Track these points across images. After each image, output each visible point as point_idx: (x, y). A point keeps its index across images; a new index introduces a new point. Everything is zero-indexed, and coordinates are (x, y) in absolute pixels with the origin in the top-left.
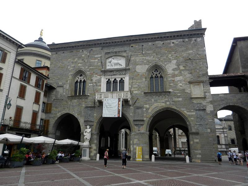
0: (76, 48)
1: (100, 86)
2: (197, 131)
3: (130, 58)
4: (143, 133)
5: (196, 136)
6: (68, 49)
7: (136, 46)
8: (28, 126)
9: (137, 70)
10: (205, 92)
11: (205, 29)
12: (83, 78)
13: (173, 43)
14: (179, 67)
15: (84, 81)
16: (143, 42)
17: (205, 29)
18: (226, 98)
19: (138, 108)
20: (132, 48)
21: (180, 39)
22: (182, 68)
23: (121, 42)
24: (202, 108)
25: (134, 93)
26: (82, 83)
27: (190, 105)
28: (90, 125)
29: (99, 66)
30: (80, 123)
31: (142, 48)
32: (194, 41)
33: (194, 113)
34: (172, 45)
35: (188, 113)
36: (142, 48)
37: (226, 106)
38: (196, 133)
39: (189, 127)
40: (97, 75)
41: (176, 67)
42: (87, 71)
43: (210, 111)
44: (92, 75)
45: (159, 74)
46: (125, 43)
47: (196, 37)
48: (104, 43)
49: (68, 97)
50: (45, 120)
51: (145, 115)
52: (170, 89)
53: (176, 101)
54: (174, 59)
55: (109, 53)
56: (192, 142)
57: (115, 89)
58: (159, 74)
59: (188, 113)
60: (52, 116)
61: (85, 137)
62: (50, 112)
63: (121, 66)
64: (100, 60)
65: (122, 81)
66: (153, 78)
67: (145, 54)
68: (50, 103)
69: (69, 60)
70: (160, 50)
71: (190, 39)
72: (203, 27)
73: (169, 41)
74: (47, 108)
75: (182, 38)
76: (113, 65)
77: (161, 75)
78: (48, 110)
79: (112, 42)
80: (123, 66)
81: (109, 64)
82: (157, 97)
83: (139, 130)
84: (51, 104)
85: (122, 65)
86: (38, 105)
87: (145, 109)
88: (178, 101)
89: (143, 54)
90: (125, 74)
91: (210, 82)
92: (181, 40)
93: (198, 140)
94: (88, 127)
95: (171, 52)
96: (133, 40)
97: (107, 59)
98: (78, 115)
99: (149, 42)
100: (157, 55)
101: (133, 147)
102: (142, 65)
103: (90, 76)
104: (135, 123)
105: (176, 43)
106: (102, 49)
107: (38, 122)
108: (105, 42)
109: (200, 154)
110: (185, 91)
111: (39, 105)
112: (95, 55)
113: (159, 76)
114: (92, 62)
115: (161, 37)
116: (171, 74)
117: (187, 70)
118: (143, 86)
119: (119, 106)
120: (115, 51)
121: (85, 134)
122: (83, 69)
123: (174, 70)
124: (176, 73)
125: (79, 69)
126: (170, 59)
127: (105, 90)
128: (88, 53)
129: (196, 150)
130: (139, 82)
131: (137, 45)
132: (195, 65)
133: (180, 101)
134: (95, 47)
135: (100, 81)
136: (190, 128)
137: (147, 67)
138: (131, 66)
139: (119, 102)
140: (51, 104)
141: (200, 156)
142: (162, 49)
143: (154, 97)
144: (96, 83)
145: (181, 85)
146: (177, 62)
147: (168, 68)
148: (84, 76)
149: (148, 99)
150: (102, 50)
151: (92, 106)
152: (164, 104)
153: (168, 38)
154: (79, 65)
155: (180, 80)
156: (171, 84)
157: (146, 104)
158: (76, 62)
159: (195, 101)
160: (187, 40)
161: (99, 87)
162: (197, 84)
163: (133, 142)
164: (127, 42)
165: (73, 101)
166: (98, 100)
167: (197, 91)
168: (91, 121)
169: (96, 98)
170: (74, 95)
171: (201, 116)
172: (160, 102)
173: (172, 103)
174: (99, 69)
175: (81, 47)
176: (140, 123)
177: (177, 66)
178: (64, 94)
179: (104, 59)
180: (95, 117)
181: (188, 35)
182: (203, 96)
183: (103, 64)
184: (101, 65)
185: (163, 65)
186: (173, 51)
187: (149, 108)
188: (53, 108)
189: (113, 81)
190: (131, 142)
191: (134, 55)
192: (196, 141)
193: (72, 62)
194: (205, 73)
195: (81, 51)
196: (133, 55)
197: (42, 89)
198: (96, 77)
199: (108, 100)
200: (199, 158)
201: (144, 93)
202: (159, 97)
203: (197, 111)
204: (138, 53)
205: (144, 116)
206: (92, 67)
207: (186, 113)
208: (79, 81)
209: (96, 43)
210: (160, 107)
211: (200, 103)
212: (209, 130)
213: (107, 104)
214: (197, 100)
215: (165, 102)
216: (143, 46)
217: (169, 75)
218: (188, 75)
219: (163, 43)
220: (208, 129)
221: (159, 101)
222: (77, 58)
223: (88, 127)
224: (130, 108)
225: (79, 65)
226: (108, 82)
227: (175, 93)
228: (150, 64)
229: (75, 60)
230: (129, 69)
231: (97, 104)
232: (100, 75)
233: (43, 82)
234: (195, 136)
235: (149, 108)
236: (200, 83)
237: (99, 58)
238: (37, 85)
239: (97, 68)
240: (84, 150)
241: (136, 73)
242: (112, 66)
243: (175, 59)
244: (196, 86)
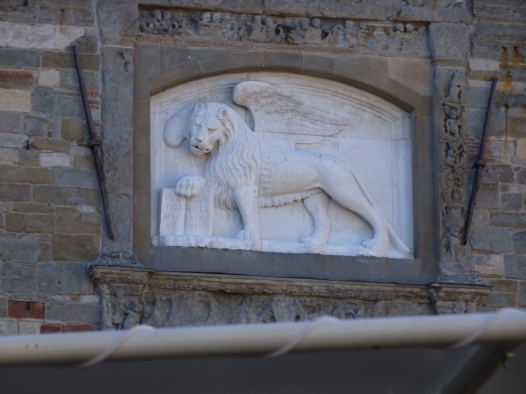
64: (72, 102)
76: (248, 197)
184: (90, 184)
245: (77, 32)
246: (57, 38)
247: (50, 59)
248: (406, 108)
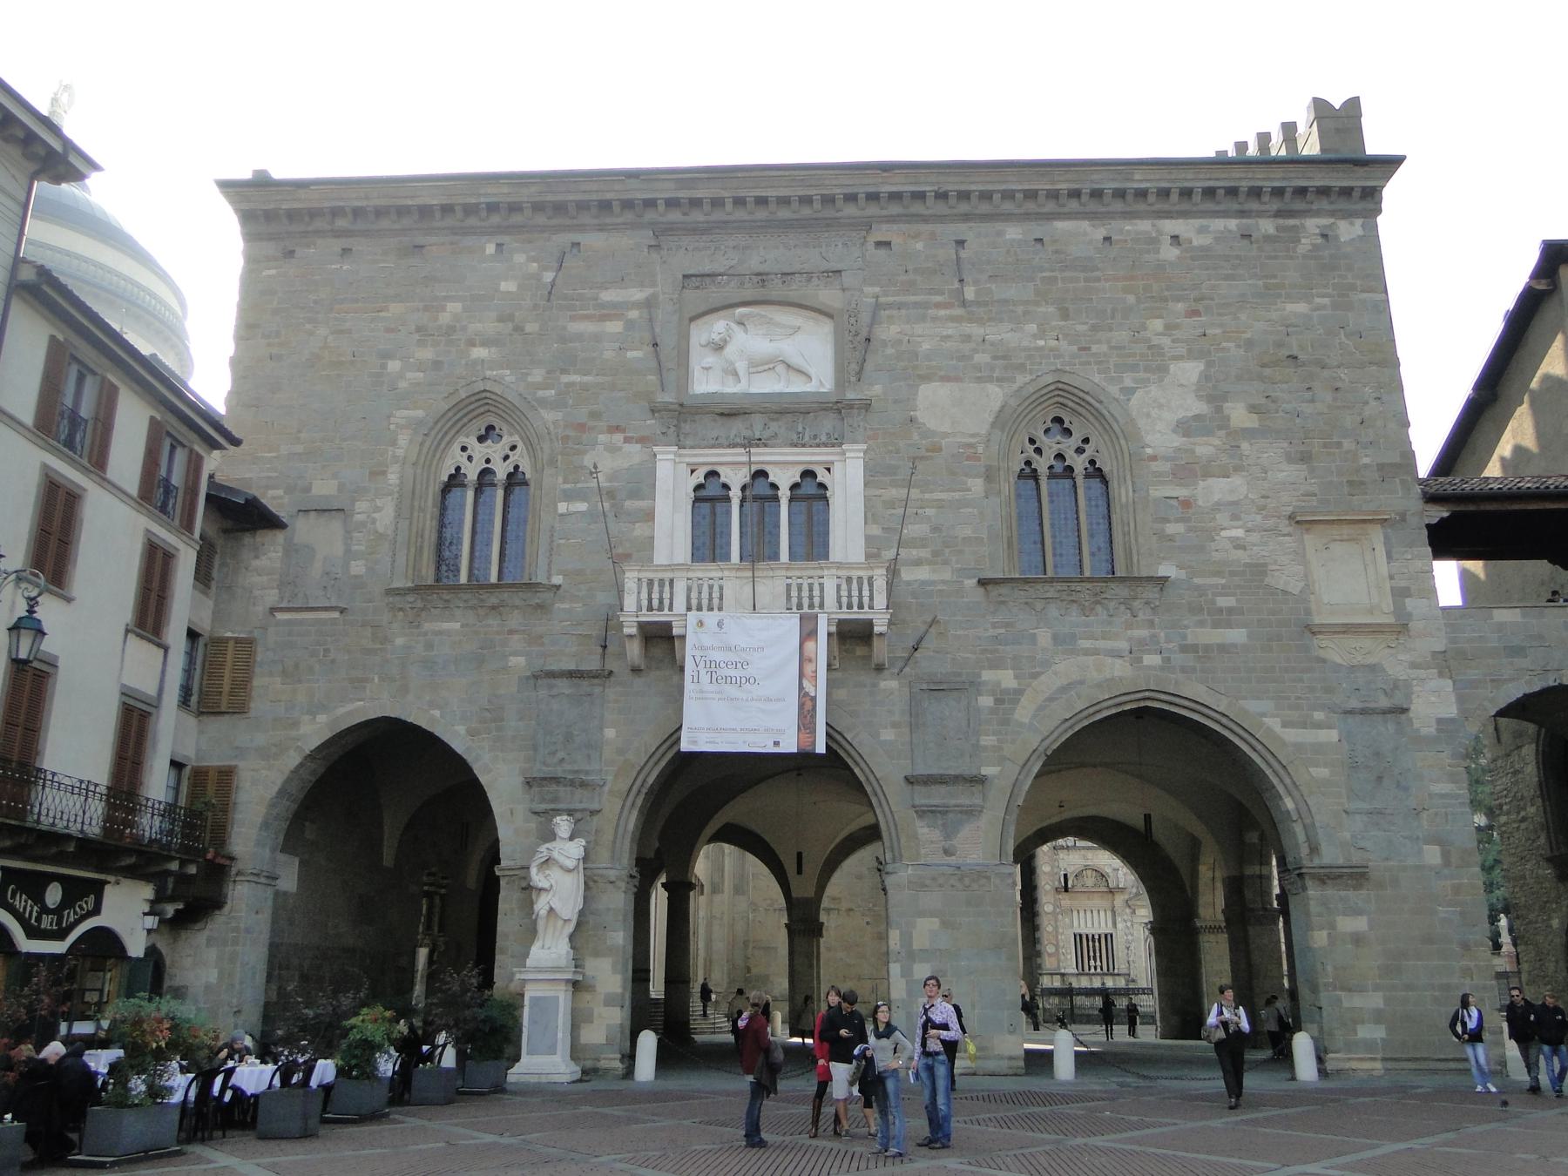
0: (449, 221)
1: (650, 516)
2: (1357, 858)
3: (871, 326)
4: (980, 874)
5: (1351, 894)
6: (385, 223)
7: (917, 243)
8: (89, 818)
9: (920, 415)
10: (1400, 594)
11: (1391, 164)
12: (506, 458)
13: (1175, 238)
14: (1219, 410)
15: (515, 480)
16: (966, 217)
17: (1391, 164)
18: (1541, 637)
19: (938, 688)
20: (882, 252)
21: (1225, 214)
22: (1239, 414)
23: (806, 200)
24: (1384, 702)
25: (909, 583)
26: (500, 493)
27: (1301, 680)
28: (570, 813)
30: (492, 796)
31: (958, 258)
32: (1320, 240)
33: (1333, 735)
34: (1170, 253)
35: (1292, 735)
36: (958, 258)
37: (1536, 688)
38: (1351, 875)
39: (1298, 828)
40: (618, 438)
41: (1201, 407)
42: (543, 402)
43: (1440, 721)
45: (1080, 451)
46: (829, 213)
47: (1332, 214)
48: (672, 203)
49: (390, 592)
50: (200, 775)
51: (988, 740)
53: (1207, 648)
54: (1182, 350)
55: (712, 275)
56: (1324, 933)
57: (760, 550)
58: (1080, 451)
59: (1292, 735)
60: (261, 739)
61: (541, 906)
62: (239, 708)
63: (793, 376)
65: (812, 492)
66: (1034, 475)
67: (978, 303)
68: (237, 641)
69: (396, 309)
70: (1086, 280)
71: (1291, 222)
72: (1374, 146)
73: (1144, 226)
74: (216, 679)
75: (1242, 214)
76: (741, 367)
77: (1092, 462)
78: (226, 688)
79: (739, 202)
80: (820, 378)
81: (710, 359)
82: (1074, 615)
83: (947, 852)
84: (246, 645)
85: (812, 371)
86: (159, 645)
87: (986, 701)
88: (1223, 648)
89: (964, 303)
90: (836, 441)
91: (1428, 526)
92: (1233, 224)
93: (1360, 924)
94: (563, 825)
95: (1166, 300)
96: (895, 197)
97: (692, 319)
98: (472, 733)
99: (1008, 217)
100: (1065, 315)
101: (907, 973)
102: (957, 379)
103: (566, 438)
104: (920, 800)
105: (1195, 243)
106: (658, 247)
107: (157, 785)
108: (682, 194)
109: (1378, 1017)
110: (1267, 580)
111: (166, 649)
112: (604, 286)
113: (1079, 464)
114: (579, 337)
115: (1097, 194)
116: (1166, 459)
118: (968, 532)
119: (809, 668)
120: (754, 263)
121: (537, 878)
122: (506, 381)
123: (1185, 427)
124: (1200, 450)
125: (480, 386)
126: (1157, 350)
127: (683, 552)
128: (546, 269)
129: (1350, 990)
130: (940, 505)
131: (916, 236)
133: (1234, 645)
134: (601, 228)
135: (642, 484)
136: (1301, 837)
137: (995, 395)
138: (877, 389)
139: (809, 645)
140: (246, 645)
141: (1378, 1033)
142: (1098, 280)
143: (1053, 611)
144: (611, 494)
145: (1240, 533)
146: (1205, 377)
147: (1148, 415)
148: (516, 439)
149: (1007, 625)
150: (655, 256)
152: (1120, 669)
153: (1141, 207)
154: (479, 353)
156: (1171, 529)
157: (995, 665)
158: (451, 329)
159: (1335, 651)
160: (1267, 226)
161: (639, 530)
162: (1346, 530)
163: (907, 938)
164: (850, 210)
165: (427, 626)
166: (642, 626)
167: (1342, 581)
168: (583, 784)
169: (630, 603)
170: (430, 581)
171: (1377, 754)
172: (1096, 652)
173: (1178, 659)
175: (495, 219)
176: (953, 802)
177: (1210, 399)
178: (357, 567)
180: (619, 755)
181: (1278, 192)
182: (1391, 620)
183: (670, 359)
184: (654, 364)
185: (1114, 390)
186: (1178, 299)
187: (1019, 692)
189: (744, 488)
190: (894, 937)
191: (900, 306)
192: (1350, 924)
193: (419, 329)
194: (1398, 460)
195: (490, 249)
196: (890, 306)
197: (188, 525)
198: (613, 449)
199: (720, 624)
200: (1369, 1045)
202: (1084, 611)
203: (1350, 719)
204: (932, 292)
205: (985, 748)
206: (576, 378)
207: (1278, 729)
208: (472, 473)
209: (609, 196)
210: (1099, 686)
211: (1373, 668)
212: (1432, 855)
213: (717, 656)
214: (1351, 642)
215: (1134, 654)
216: (961, 243)
217: (1154, 466)
219: (1107, 239)
220: (1425, 847)
221: (1085, 644)
222: (447, 298)
223: (563, 825)
224: (874, 685)
225: (479, 353)
226: (708, 496)
227: (1198, 587)
228: (1021, 379)
229: (445, 318)
230: (866, 406)
231: (634, 650)
232: (642, 440)
233: (195, 464)
234: (1342, 893)
235: (1019, 692)
236: (1369, 527)
237: (634, 314)
238: (155, 493)
240: (535, 1000)
241: (916, 436)
242: (735, 374)
243: (1191, 355)
244: (1338, 548)
245: (651, 291)
246: (638, 295)
248: (830, 316)
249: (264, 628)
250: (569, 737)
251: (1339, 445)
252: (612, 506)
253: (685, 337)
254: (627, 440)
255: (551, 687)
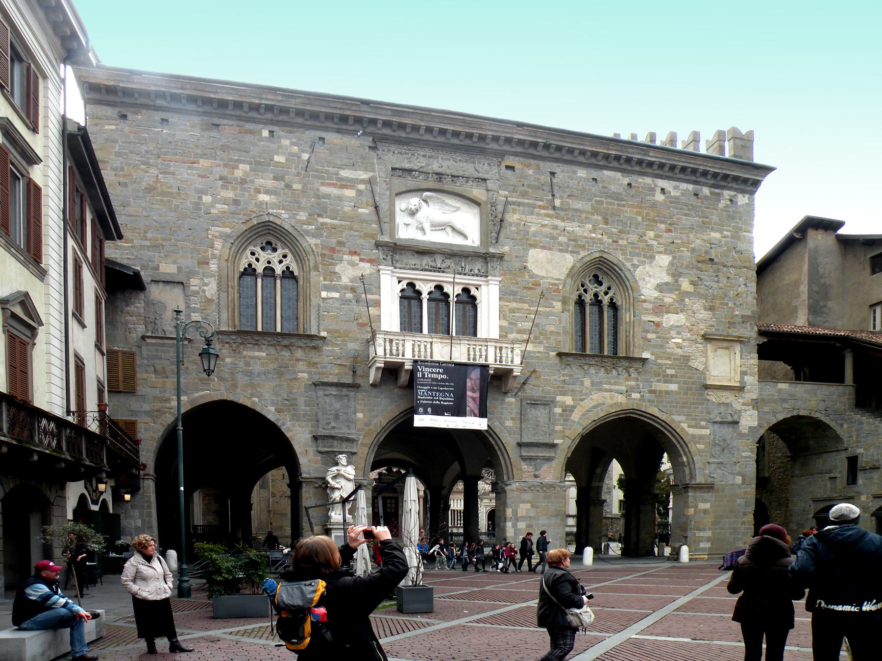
29: (366, 221)
44: (331, 254)
52: (643, 350)
81: (408, 220)
98: (278, 411)
117: (702, 295)
132: (725, 282)
151: (343, 381)
155: (678, 326)
156: (650, 336)
174: (366, 235)
179: (388, 193)
184: (375, 218)
188: (145, 375)
201: (560, 355)
202: (607, 372)
218: (702, 311)
232: (370, 261)
239: (356, 226)
247: (362, 181)
249: (139, 347)
250: (337, 417)
251: (727, 304)
252: (354, 296)
253: (392, 205)
254: (361, 260)
255: (324, 390)
